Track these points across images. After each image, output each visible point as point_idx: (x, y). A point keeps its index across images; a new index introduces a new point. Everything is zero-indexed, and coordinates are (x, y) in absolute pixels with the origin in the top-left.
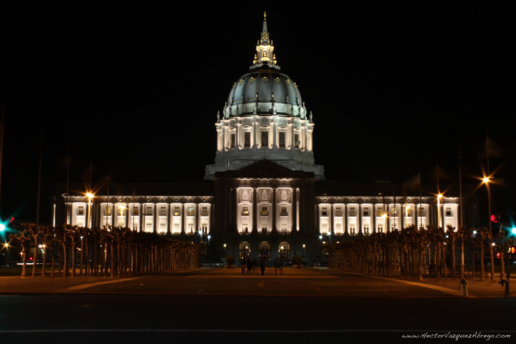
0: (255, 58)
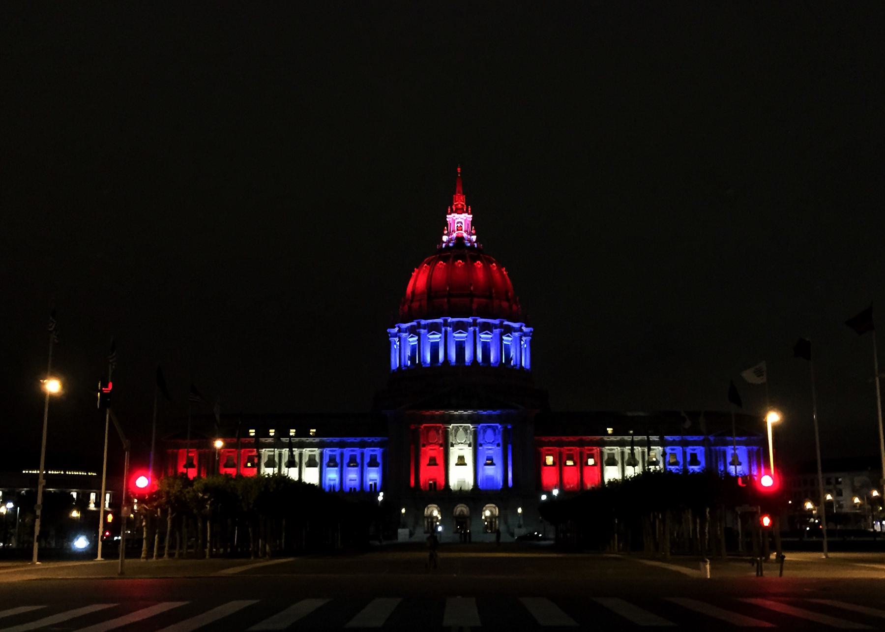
0: (446, 232)
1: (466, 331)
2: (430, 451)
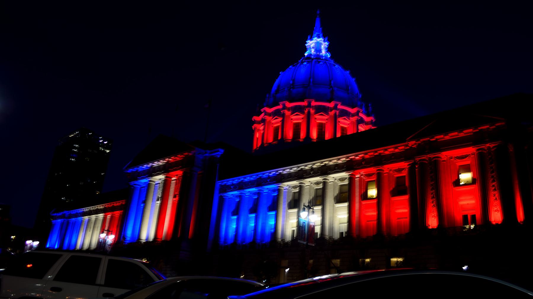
1: (328, 114)
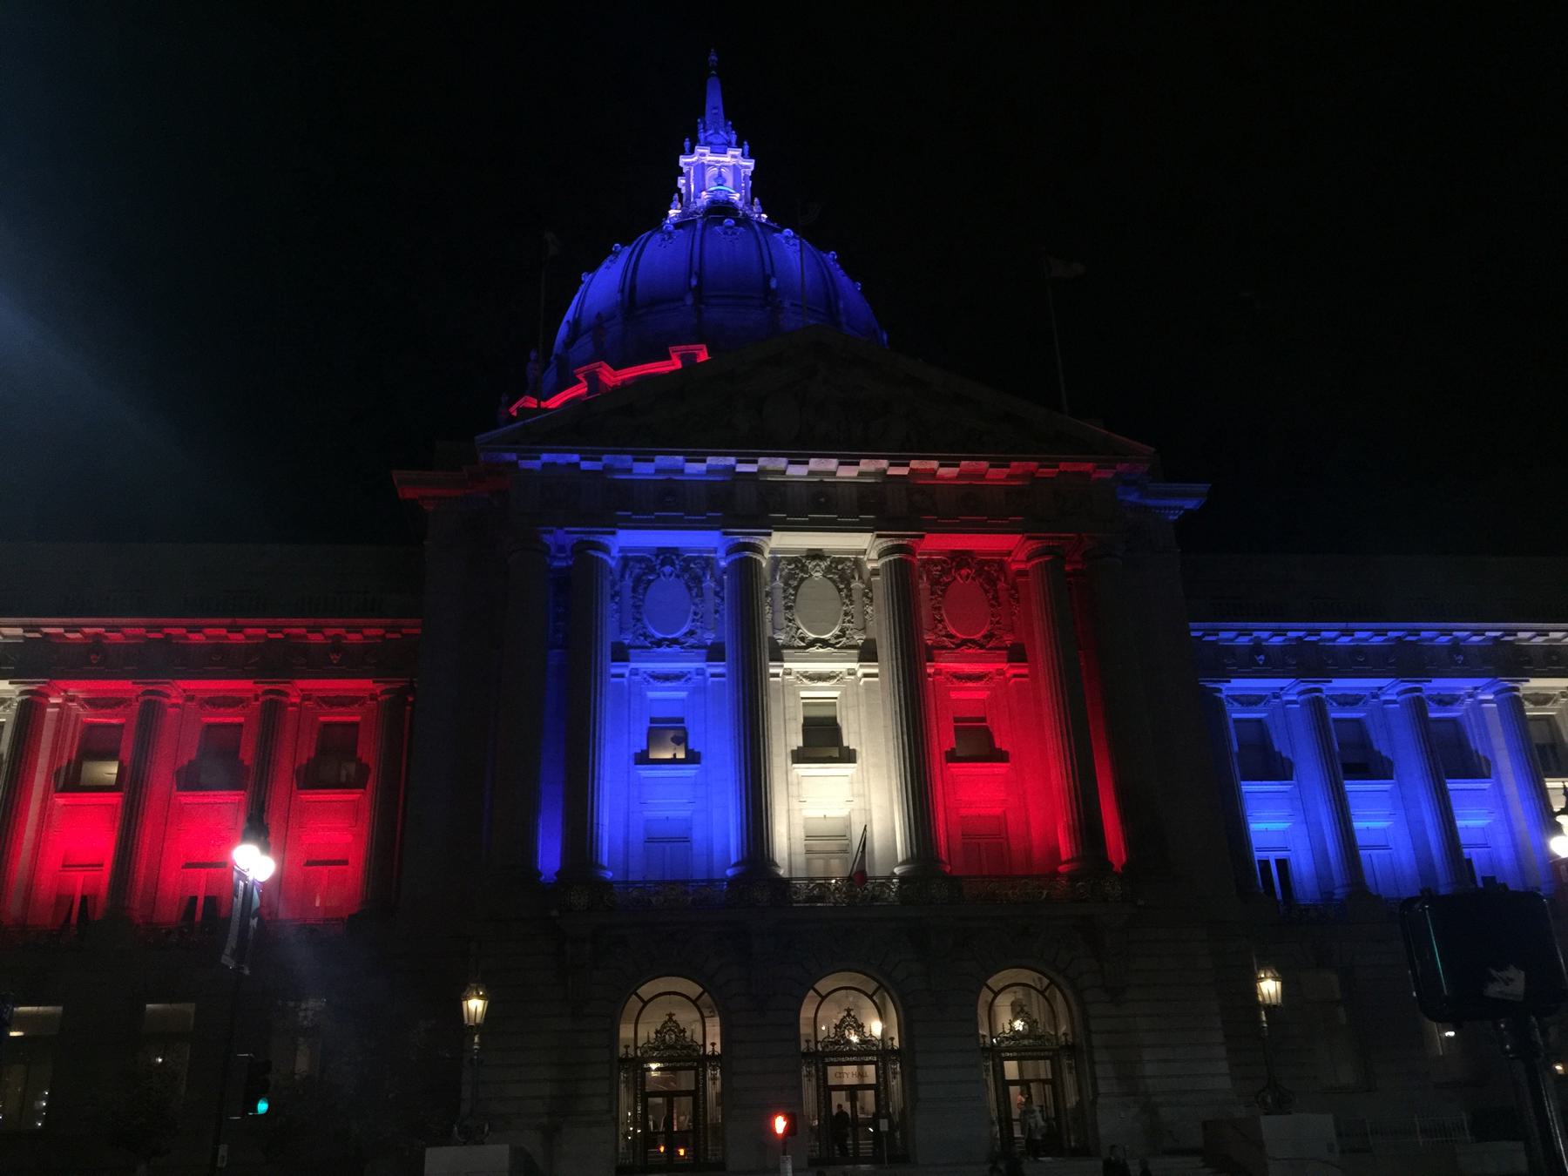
2: (660, 679)
